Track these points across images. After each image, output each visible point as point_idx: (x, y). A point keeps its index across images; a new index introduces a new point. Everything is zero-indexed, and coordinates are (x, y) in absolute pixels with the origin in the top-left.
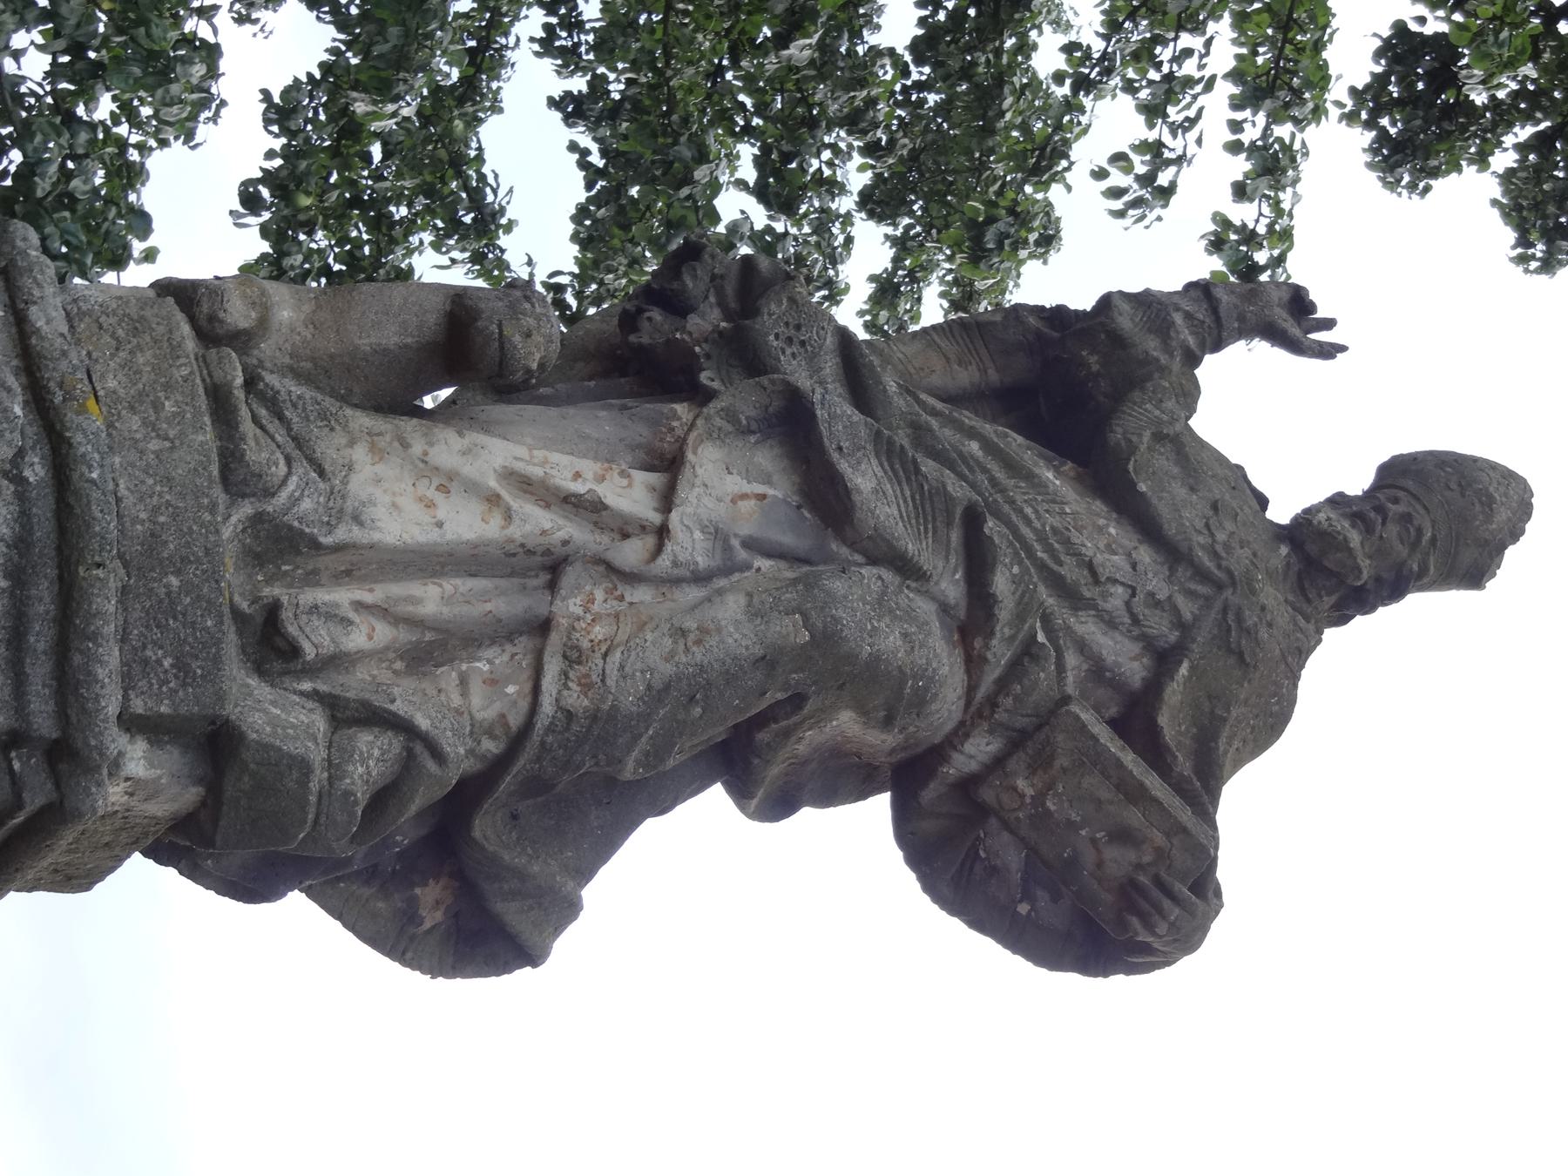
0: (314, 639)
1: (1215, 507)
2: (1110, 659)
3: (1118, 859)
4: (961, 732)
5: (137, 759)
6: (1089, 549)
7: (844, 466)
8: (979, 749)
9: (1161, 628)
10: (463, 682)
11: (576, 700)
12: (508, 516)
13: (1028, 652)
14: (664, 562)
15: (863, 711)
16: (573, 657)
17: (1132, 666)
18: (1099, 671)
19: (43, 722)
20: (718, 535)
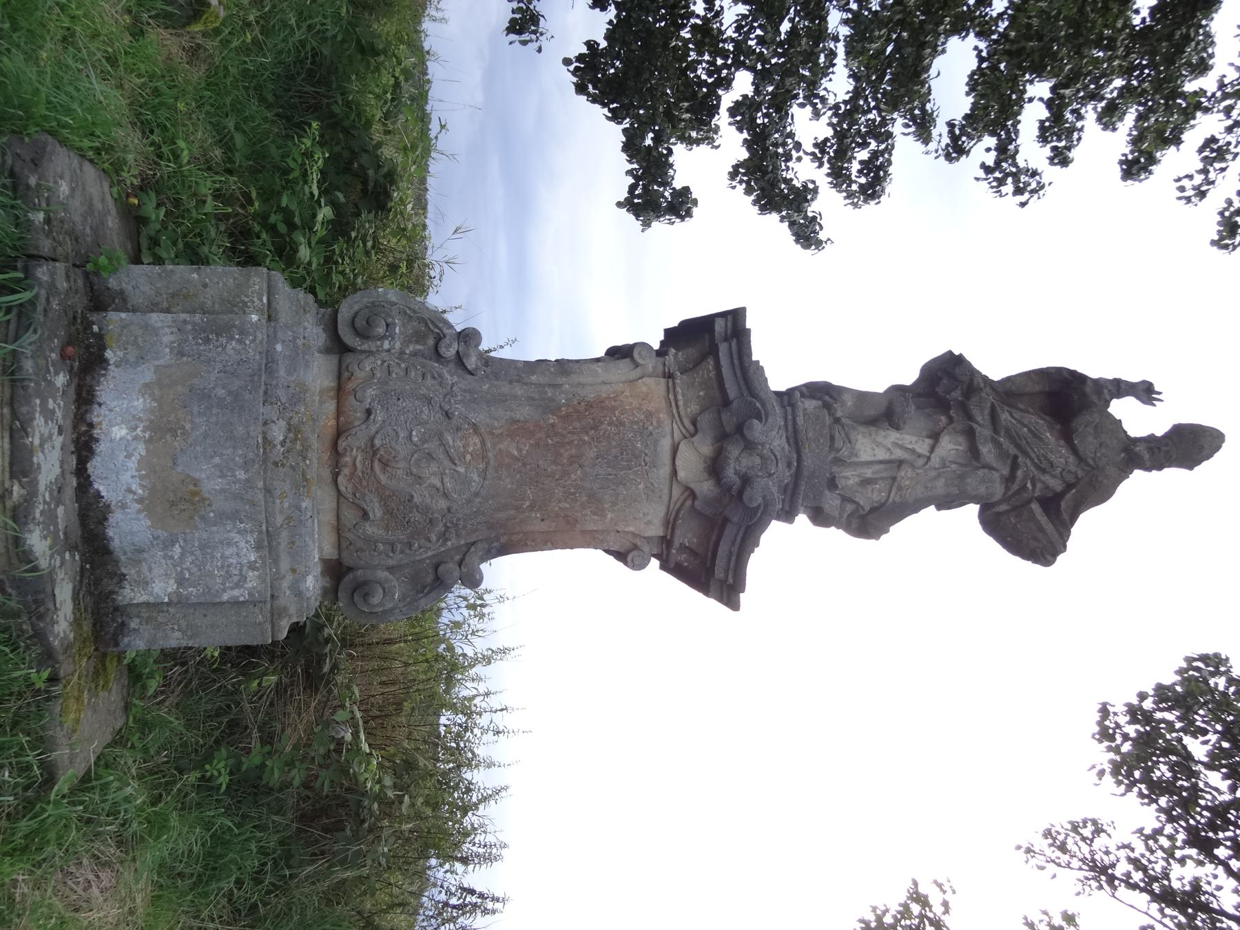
1: (1101, 445)
2: (1051, 485)
8: (1003, 507)
9: (1071, 479)
12: (891, 453)
16: (900, 488)
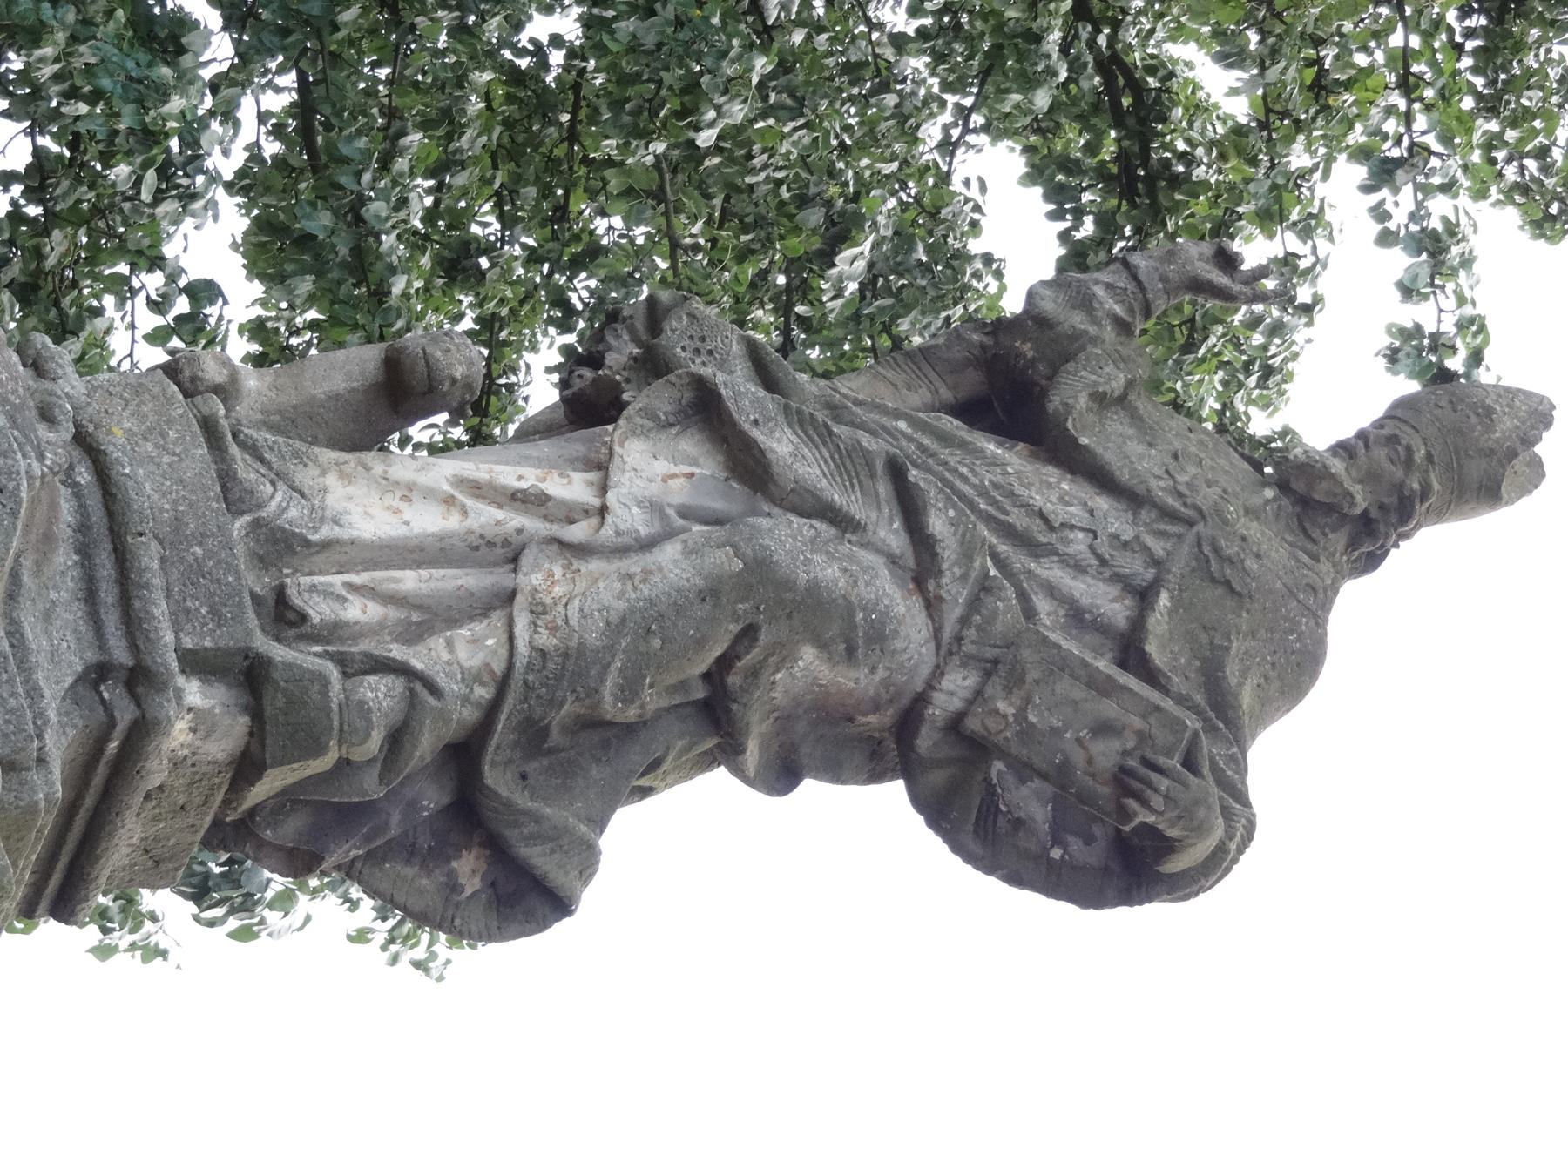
0: (319, 611)
2: (1085, 601)
3: (1106, 753)
4: (938, 672)
5: (194, 693)
6: (1038, 500)
7: (756, 433)
9: (1133, 565)
10: (450, 644)
11: (545, 639)
12: (464, 512)
13: (985, 587)
14: (608, 531)
15: (823, 645)
16: (538, 611)
17: (1115, 609)
18: (1078, 617)
19: (120, 653)
20: (654, 508)
